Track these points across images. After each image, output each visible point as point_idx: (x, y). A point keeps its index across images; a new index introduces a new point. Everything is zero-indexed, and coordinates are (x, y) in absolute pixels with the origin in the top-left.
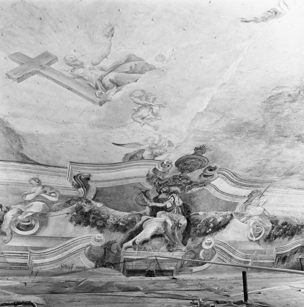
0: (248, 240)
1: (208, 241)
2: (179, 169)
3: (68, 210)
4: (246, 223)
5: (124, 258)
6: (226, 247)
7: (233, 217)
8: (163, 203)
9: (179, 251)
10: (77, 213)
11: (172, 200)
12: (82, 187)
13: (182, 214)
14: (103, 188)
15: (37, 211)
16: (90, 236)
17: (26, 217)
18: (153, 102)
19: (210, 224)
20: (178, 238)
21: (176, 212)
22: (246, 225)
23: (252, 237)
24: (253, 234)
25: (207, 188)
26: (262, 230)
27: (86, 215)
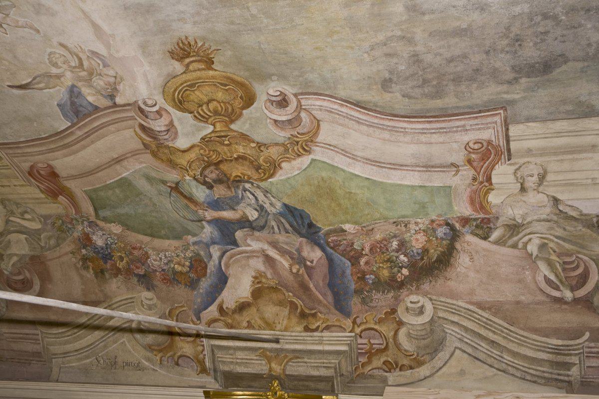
0: (543, 298)
1: (411, 302)
2: (195, 116)
3: (67, 247)
4: (515, 246)
5: (212, 346)
6: (476, 319)
7: (459, 231)
8: (235, 210)
9: (333, 329)
10: (86, 251)
11: (249, 198)
12: (61, 195)
13: (296, 234)
14: (95, 190)
15: (23, 252)
16: (131, 298)
17: (13, 265)
19: (397, 257)
20: (321, 297)
21: (279, 229)
22: (516, 252)
23: (557, 288)
24: (552, 277)
25: (318, 154)
26: (585, 265)
27: (105, 255)
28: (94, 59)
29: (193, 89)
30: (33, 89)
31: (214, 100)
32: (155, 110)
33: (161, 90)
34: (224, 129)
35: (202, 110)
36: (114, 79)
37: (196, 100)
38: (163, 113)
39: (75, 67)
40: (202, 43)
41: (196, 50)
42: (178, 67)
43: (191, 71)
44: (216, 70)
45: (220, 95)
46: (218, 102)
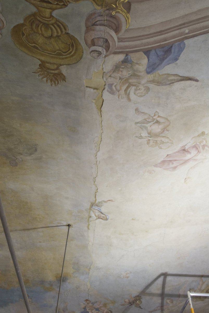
2: (65, 29)
18: (149, 140)
28: (116, 89)
29: (60, 51)
30: (181, 77)
31: (46, 38)
32: (95, 47)
33: (82, 60)
34: (43, 9)
35: (58, 32)
36: (112, 75)
37: (60, 42)
38: (89, 42)
39: (135, 85)
40: (44, 79)
41: (48, 76)
42: (64, 70)
43: (56, 64)
44: (39, 59)
45: (41, 40)
46: (43, 35)
